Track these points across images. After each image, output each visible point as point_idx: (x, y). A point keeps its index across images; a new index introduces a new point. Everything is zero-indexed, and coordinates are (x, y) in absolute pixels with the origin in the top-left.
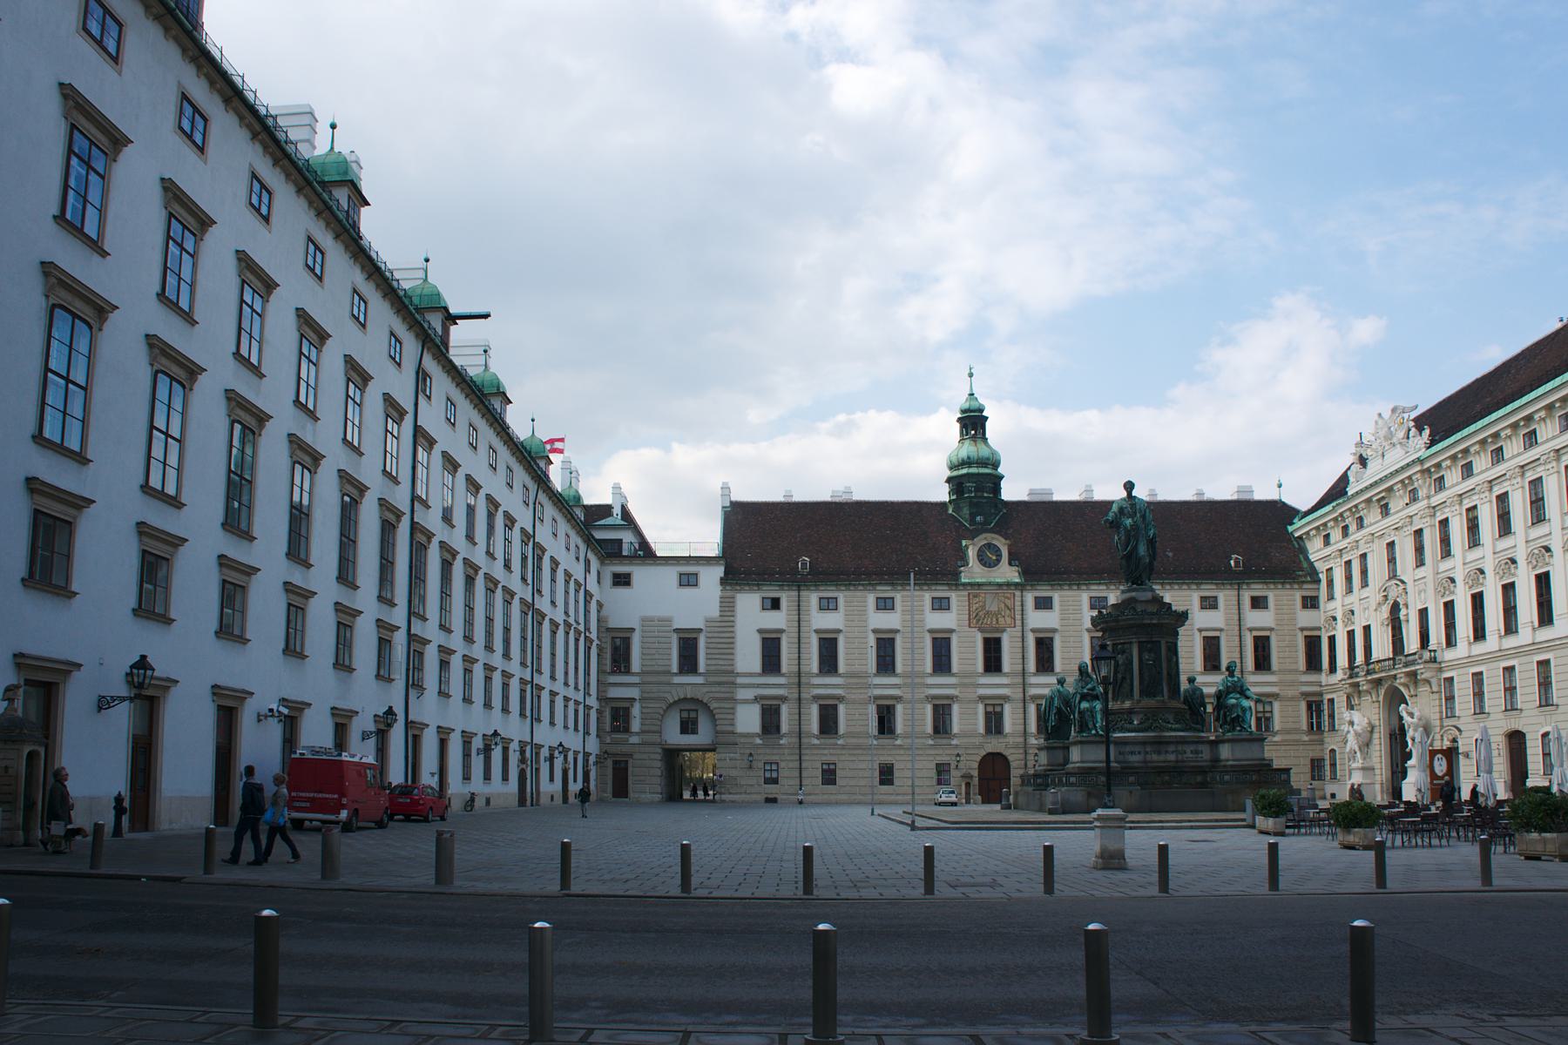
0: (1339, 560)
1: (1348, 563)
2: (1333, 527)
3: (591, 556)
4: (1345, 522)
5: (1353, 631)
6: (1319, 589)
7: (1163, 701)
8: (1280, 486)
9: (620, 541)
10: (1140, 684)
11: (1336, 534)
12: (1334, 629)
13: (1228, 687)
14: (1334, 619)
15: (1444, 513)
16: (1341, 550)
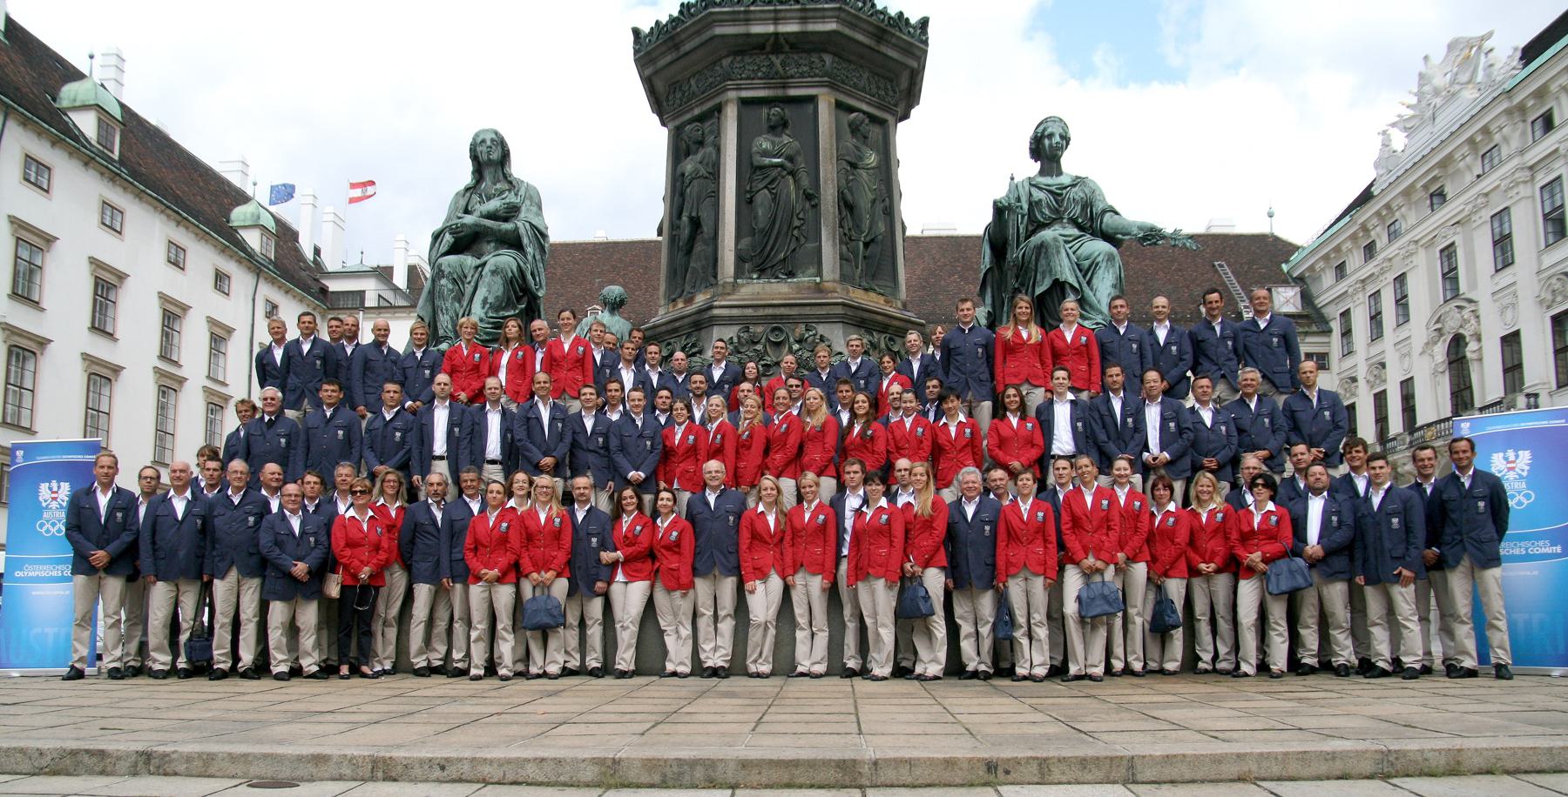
0: (1360, 295)
1: (1376, 295)
2: (1350, 250)
3: (266, 291)
4: (1370, 236)
5: (1384, 391)
6: (1329, 343)
7: (818, 289)
8: (1271, 215)
9: (361, 294)
10: (738, 237)
11: (1355, 260)
12: (1354, 395)
13: (1034, 205)
14: (1354, 380)
15: (1552, 170)
16: (1363, 281)
